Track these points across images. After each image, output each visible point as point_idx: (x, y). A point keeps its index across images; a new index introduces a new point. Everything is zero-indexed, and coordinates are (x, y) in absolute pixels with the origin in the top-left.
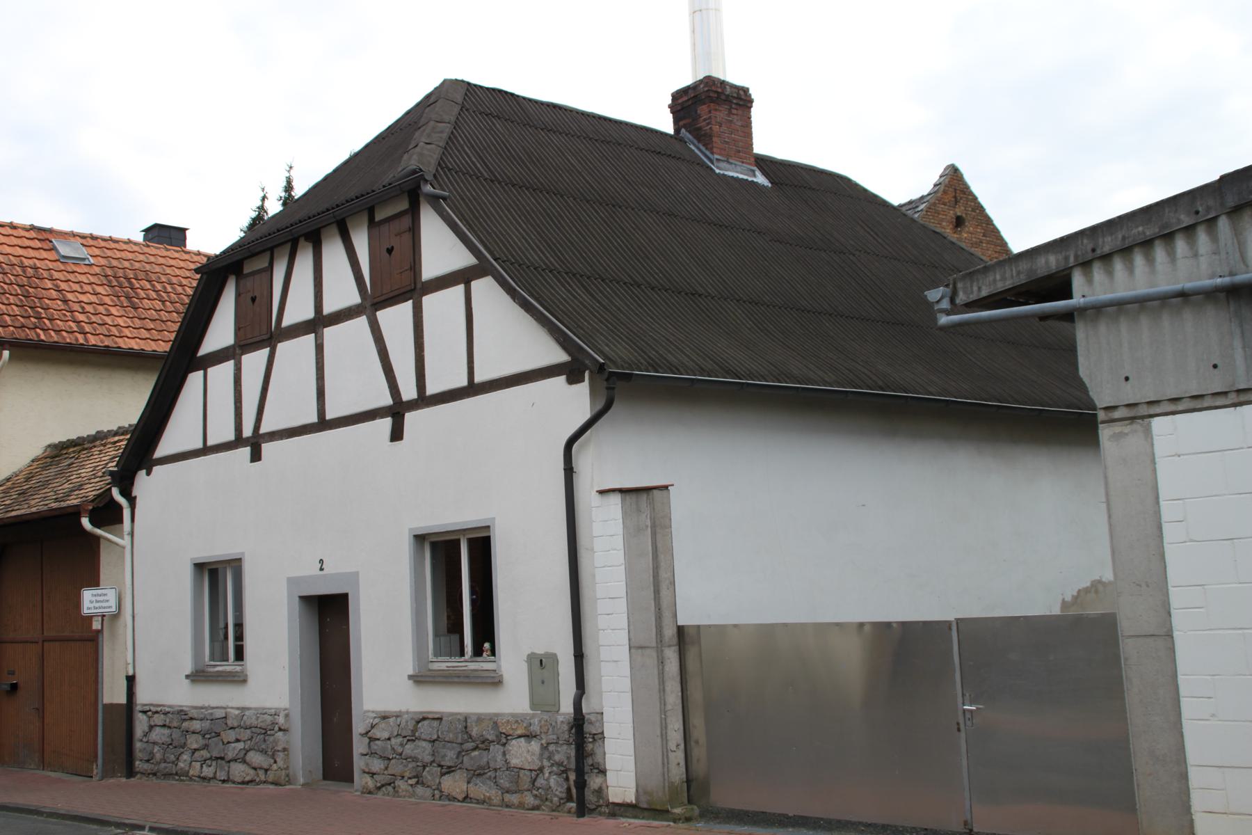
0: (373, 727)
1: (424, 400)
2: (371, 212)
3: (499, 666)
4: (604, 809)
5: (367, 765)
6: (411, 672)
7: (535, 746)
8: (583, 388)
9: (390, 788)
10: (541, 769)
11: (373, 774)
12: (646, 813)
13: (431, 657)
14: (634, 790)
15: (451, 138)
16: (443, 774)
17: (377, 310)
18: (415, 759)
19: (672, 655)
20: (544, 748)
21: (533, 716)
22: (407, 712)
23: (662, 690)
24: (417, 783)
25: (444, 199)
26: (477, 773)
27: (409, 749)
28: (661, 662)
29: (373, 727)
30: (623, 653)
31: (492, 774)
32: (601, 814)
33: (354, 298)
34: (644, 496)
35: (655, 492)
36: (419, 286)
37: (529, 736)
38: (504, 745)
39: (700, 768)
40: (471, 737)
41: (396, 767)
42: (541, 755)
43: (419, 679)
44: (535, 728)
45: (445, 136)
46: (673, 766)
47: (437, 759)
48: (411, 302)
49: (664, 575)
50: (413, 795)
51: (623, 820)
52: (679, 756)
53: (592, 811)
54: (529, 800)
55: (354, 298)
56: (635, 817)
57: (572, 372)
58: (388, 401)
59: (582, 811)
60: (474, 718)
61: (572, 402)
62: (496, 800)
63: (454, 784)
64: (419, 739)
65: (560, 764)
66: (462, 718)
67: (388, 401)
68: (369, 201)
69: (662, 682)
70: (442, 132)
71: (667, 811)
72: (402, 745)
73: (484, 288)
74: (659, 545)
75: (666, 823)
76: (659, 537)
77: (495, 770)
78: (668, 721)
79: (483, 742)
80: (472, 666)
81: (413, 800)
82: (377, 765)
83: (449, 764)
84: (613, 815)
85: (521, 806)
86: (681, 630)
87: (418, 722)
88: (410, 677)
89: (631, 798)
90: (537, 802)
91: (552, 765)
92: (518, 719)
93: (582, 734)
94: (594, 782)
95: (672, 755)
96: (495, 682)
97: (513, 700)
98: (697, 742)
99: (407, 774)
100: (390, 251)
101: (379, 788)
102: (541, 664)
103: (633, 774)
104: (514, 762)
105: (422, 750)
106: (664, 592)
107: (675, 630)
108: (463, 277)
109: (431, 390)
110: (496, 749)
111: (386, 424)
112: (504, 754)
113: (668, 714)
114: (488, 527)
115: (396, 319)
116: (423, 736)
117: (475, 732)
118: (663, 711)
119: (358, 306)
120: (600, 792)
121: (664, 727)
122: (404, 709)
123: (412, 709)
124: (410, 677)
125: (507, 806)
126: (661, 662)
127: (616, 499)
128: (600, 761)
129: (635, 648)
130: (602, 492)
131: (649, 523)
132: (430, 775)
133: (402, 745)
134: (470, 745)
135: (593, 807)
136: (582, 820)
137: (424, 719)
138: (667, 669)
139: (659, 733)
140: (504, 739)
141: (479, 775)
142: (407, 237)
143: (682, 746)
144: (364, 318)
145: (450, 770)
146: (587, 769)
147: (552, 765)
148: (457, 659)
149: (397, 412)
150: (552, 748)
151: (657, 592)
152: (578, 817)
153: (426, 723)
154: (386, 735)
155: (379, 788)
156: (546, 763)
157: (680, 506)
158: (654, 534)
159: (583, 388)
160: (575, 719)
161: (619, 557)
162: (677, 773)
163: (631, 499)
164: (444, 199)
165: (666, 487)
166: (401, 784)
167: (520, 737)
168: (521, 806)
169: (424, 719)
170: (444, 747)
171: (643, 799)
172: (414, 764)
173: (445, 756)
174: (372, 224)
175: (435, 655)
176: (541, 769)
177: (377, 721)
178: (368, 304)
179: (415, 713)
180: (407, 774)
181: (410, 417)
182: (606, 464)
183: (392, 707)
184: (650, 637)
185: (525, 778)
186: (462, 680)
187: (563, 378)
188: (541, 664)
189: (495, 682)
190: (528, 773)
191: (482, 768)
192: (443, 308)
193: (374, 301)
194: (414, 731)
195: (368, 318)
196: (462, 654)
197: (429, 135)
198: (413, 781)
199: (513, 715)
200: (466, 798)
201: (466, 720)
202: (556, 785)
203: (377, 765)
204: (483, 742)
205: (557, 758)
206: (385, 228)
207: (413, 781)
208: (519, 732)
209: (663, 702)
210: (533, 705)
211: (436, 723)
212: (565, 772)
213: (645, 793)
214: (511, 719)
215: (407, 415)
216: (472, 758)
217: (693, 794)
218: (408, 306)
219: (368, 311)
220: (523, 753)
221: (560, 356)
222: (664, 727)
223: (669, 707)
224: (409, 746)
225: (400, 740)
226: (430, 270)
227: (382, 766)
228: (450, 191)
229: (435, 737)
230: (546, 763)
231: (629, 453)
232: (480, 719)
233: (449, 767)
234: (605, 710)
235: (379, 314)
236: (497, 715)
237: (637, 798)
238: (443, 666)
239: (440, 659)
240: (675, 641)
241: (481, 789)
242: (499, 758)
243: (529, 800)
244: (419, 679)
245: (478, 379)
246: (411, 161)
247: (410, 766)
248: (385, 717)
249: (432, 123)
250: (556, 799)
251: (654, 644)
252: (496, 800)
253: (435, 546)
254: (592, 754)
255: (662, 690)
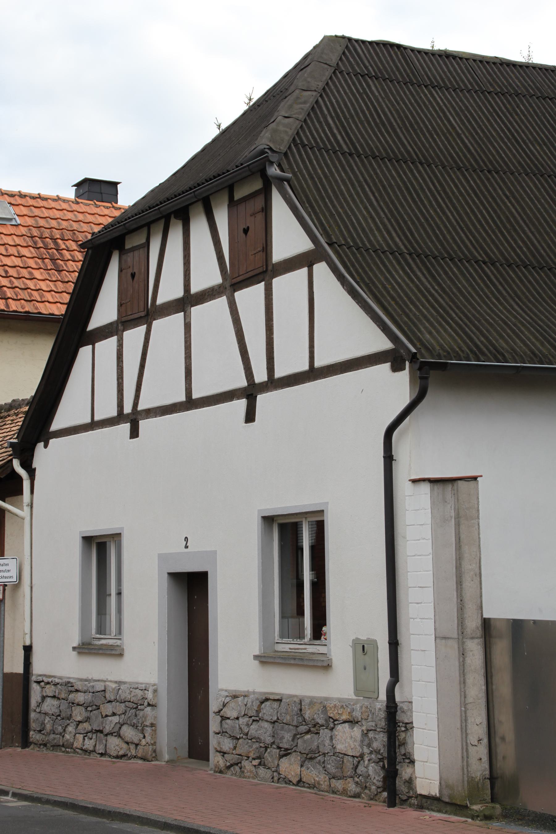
0: (224, 705)
1: (274, 383)
2: (231, 190)
3: (329, 650)
4: (414, 801)
5: (219, 743)
6: (257, 653)
7: (357, 732)
8: (404, 376)
9: (237, 768)
10: (362, 756)
11: (224, 753)
12: (448, 808)
13: (277, 639)
14: (437, 783)
15: (315, 107)
16: (281, 757)
17: (235, 291)
18: (258, 740)
19: (475, 649)
20: (365, 734)
21: (357, 702)
22: (254, 693)
23: (463, 682)
24: (260, 764)
25: (288, 181)
26: (309, 757)
27: (254, 730)
28: (463, 654)
29: (224, 705)
30: (430, 642)
31: (320, 758)
32: (411, 805)
33: (216, 279)
34: (449, 487)
35: (459, 482)
36: (270, 268)
37: (352, 722)
38: (332, 729)
39: (508, 762)
40: (304, 720)
41: (243, 747)
42: (362, 741)
43: (265, 660)
44: (357, 714)
45: (308, 106)
46: (473, 761)
47: (277, 741)
48: (263, 283)
49: (468, 566)
50: (256, 776)
51: (428, 812)
52: (482, 751)
53: (403, 802)
54: (352, 787)
55: (216, 279)
56: (439, 811)
57: (395, 359)
58: (243, 383)
59: (392, 802)
60: (307, 701)
61: (393, 388)
62: (324, 786)
63: (290, 767)
64: (262, 719)
65: (377, 752)
66: (297, 700)
67: (243, 383)
68: (226, 178)
69: (463, 673)
70: (305, 103)
71: (466, 807)
72: (248, 725)
73: (321, 269)
74: (462, 536)
75: (464, 819)
76: (462, 527)
77: (324, 754)
78: (469, 713)
79: (315, 726)
80: (311, 649)
81: (256, 781)
82: (227, 744)
83: (286, 746)
84: (421, 807)
85: (344, 792)
86: (486, 624)
87: (262, 703)
88: (256, 657)
89: (435, 791)
90: (358, 790)
91: (371, 753)
92: (344, 704)
93: (394, 723)
94: (405, 772)
95: (472, 750)
96: (324, 666)
97: (338, 686)
98: (503, 739)
99: (252, 755)
100: (246, 231)
101: (228, 768)
102: (363, 648)
103: (437, 766)
104: (340, 747)
105: (263, 730)
106: (469, 585)
107: (479, 622)
108: (305, 261)
109: (279, 373)
110: (324, 732)
111: (241, 404)
112: (331, 738)
113: (469, 706)
114: (322, 511)
115: (250, 298)
116: (266, 717)
117: (307, 715)
118: (464, 704)
119: (220, 286)
120: (410, 782)
121: (464, 720)
122: (251, 690)
123: (258, 690)
124: (256, 657)
125: (334, 792)
126: (463, 654)
127: (426, 488)
128: (411, 750)
129: (440, 638)
130: (414, 481)
131: (453, 514)
132: (271, 755)
133: (248, 725)
134: (303, 728)
135: (405, 798)
136: (391, 809)
137: (267, 700)
138: (468, 661)
139: (459, 726)
140: (332, 723)
141: (311, 759)
142: (260, 217)
143: (485, 741)
144: (224, 298)
145: (286, 753)
146: (399, 758)
147: (371, 753)
148: (299, 641)
149: (250, 393)
150: (371, 735)
151: (459, 583)
152: (389, 806)
153: (268, 703)
154: (234, 714)
155: (228, 768)
156: (366, 750)
157: (490, 498)
158: (458, 525)
159: (404, 376)
160: (387, 707)
161: (427, 547)
162: (479, 768)
163: (438, 488)
164: (288, 181)
165: (475, 478)
166: (246, 764)
167: (345, 722)
168: (344, 792)
169: (267, 700)
170: (282, 729)
171: (446, 792)
172: (256, 745)
173: (283, 738)
174: (232, 204)
175: (282, 636)
176: (362, 756)
177: (228, 699)
178: (228, 285)
179: (261, 693)
180: (252, 755)
181: (261, 399)
182: (429, 449)
183: (241, 686)
184: (452, 629)
185: (349, 763)
186: (297, 662)
187: (387, 366)
188: (363, 648)
189: (324, 666)
190: (351, 759)
191: (312, 751)
192: (289, 288)
193: (234, 281)
194: (258, 711)
195: (228, 298)
196: (301, 636)
197: (291, 107)
198: (256, 762)
199: (340, 700)
200: (300, 782)
201: (301, 704)
202: (374, 772)
203: (227, 744)
204: (315, 726)
205: (375, 745)
206: (242, 208)
207: (256, 762)
208: (344, 717)
209: (464, 695)
210: (357, 691)
211: (276, 705)
212: (381, 760)
213: (448, 786)
214: (338, 704)
215: (259, 397)
216: (305, 742)
217: (496, 791)
218: (261, 287)
219: (228, 292)
220: (347, 739)
221: (383, 344)
222: (464, 720)
223: (470, 700)
224: (254, 726)
225: (246, 719)
226: (280, 252)
227: (231, 746)
228: (294, 174)
229: (275, 718)
230: (366, 750)
231: (444, 441)
232: (312, 702)
233: (286, 749)
234: (415, 699)
235: (237, 294)
236: (327, 699)
237: (440, 791)
238: (286, 648)
239: (285, 640)
240: (479, 633)
241: (313, 774)
242: (327, 742)
243: (352, 787)
244: (265, 660)
245: (318, 363)
246: (264, 140)
247: (254, 746)
248: (235, 697)
249: (297, 92)
250: (374, 787)
251: (455, 636)
252: (324, 786)
253: (282, 527)
254: (403, 744)
255: (463, 682)
